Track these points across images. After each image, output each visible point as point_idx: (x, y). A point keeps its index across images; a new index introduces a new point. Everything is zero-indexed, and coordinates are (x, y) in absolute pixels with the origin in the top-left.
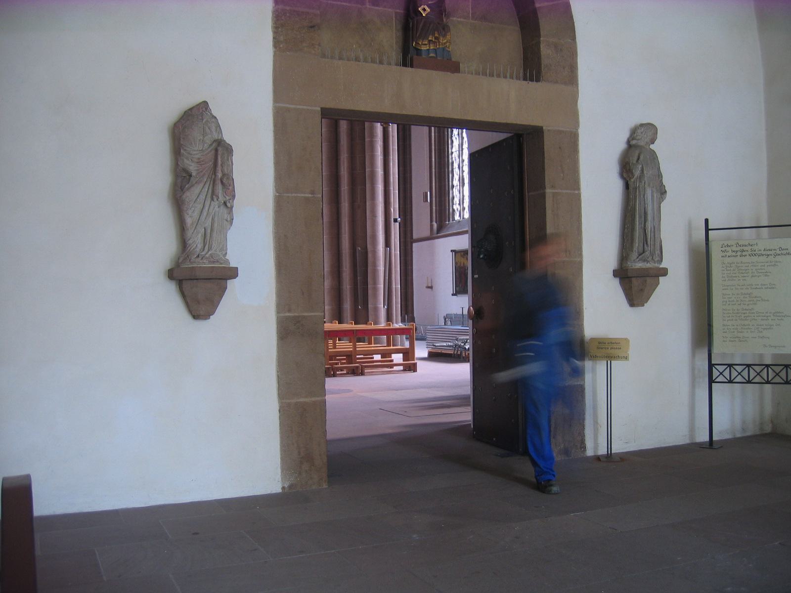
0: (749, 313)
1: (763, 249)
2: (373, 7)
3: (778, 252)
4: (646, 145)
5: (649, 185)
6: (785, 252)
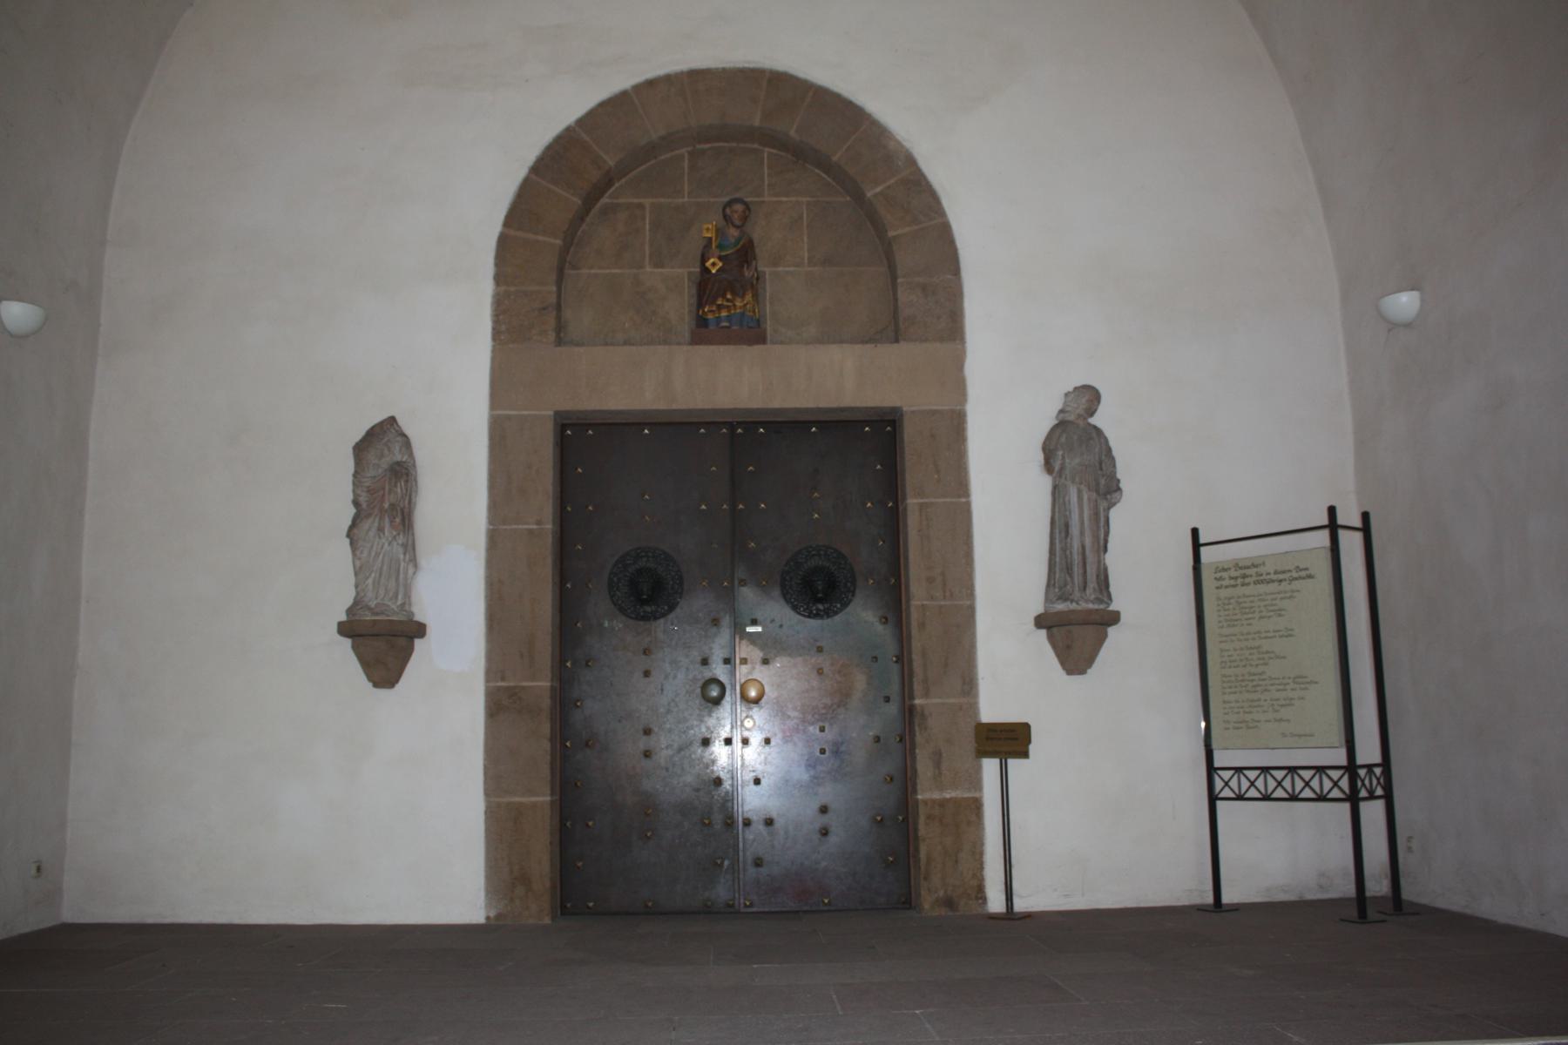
0: (1260, 680)
1: (1272, 572)
2: (656, 270)
3: (1295, 575)
4: (1077, 419)
6: (1303, 574)
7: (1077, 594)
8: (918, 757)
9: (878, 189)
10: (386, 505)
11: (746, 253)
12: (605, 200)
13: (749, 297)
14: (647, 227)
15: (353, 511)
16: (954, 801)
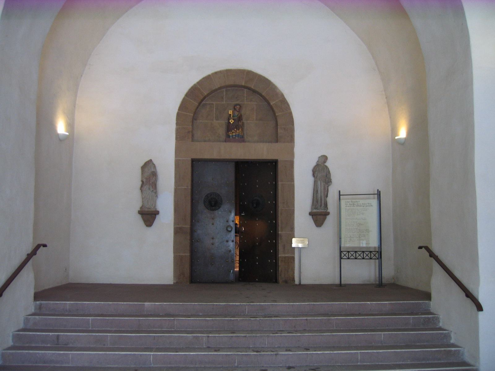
5: (319, 180)
7: (319, 207)
8: (279, 246)
9: (274, 103)
10: (151, 183)
11: (240, 118)
12: (204, 102)
13: (240, 130)
14: (214, 110)
15: (141, 183)
16: (288, 257)
